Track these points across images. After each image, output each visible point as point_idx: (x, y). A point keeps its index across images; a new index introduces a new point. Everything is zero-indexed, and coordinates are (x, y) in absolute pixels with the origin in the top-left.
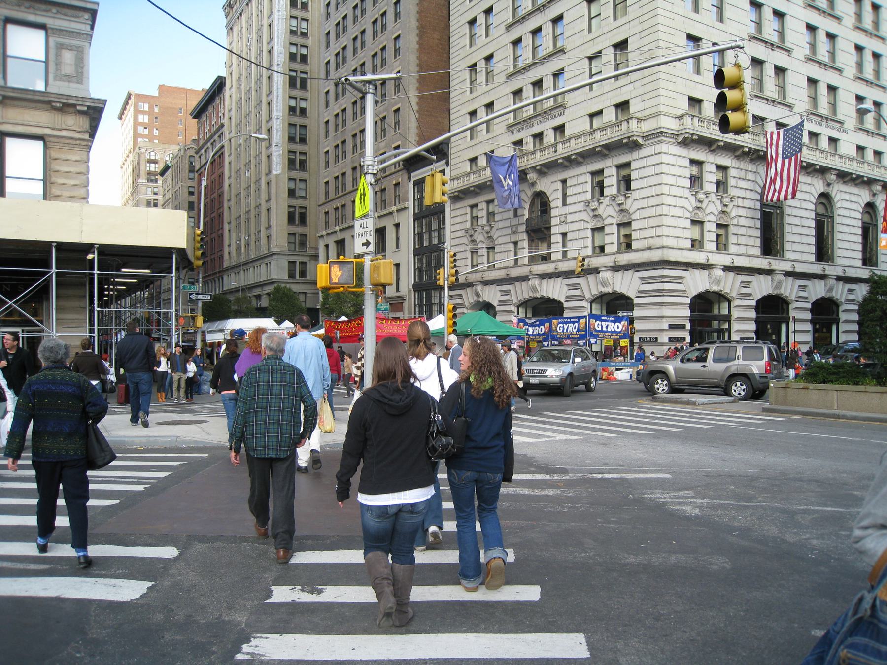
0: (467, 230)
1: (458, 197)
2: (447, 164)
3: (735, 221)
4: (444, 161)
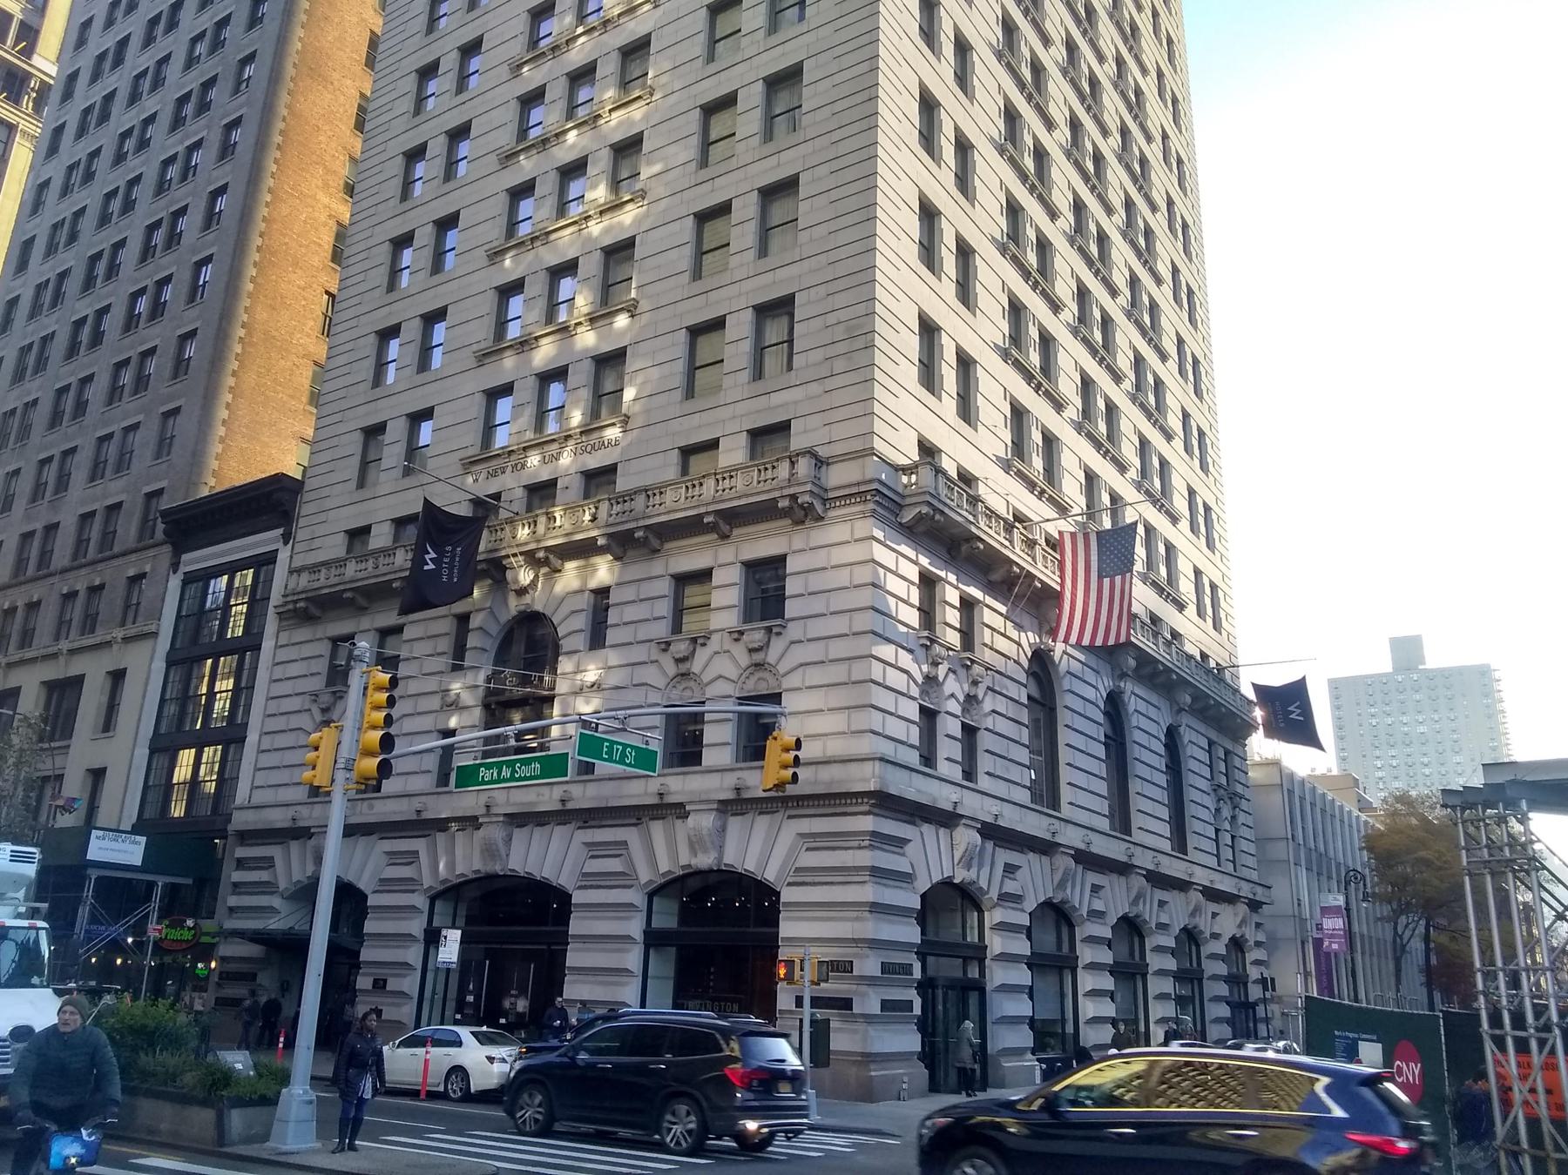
0: (315, 696)
1: (309, 610)
2: (286, 538)
3: (989, 722)
4: (281, 531)
